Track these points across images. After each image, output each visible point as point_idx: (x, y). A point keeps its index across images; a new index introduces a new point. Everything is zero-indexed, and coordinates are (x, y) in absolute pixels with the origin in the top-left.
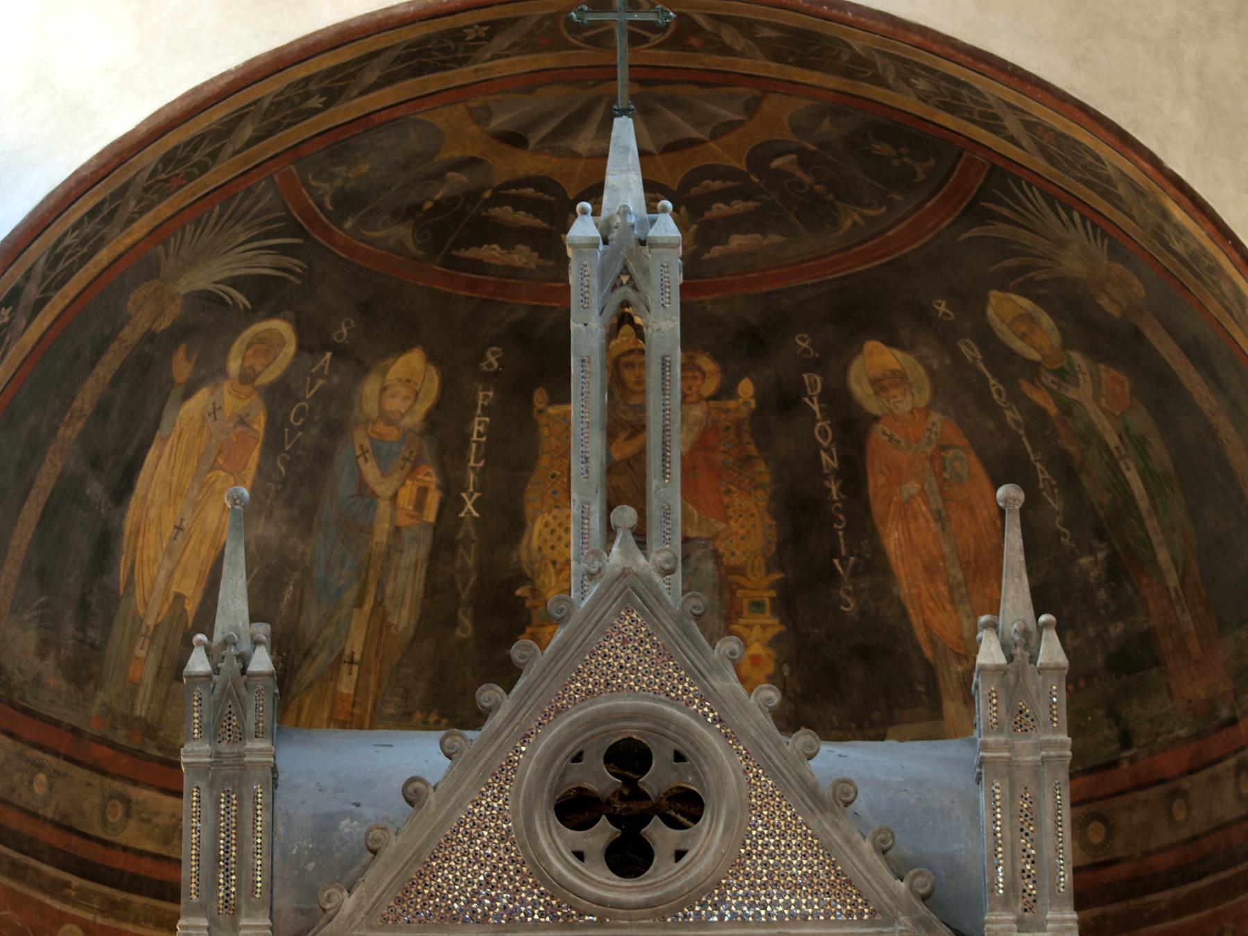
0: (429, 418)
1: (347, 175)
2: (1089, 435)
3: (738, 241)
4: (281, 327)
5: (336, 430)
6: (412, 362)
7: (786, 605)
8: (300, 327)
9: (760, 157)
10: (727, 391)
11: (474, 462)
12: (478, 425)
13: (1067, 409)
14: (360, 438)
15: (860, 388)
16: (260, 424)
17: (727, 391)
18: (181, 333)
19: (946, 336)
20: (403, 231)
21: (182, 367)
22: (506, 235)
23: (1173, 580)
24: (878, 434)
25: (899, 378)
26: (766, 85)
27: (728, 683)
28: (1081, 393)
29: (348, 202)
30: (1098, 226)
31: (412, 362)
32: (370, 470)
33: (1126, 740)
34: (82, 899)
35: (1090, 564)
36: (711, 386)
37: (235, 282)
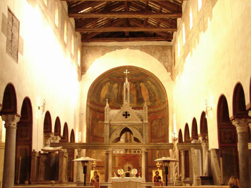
0: (117, 87)
1: (113, 75)
2: (153, 89)
3: (134, 78)
4: (109, 83)
5: (112, 87)
6: (116, 84)
7: (137, 96)
8: (110, 82)
9: (135, 74)
10: (133, 85)
11: (120, 89)
12: (120, 87)
13: (152, 87)
14: (113, 88)
15: (141, 85)
16: (108, 88)
17: (133, 85)
18: (104, 83)
19: (145, 83)
20: (116, 78)
21: (104, 85)
22: (121, 78)
23: (157, 96)
24: (142, 88)
25: (143, 85)
26: (135, 71)
27: (131, 109)
28: (152, 86)
29: (113, 76)
30: (152, 78)
31: (116, 84)
32: (114, 90)
33: (155, 104)
34: (99, 113)
35: (153, 95)
36: (132, 85)
37: (107, 81)
